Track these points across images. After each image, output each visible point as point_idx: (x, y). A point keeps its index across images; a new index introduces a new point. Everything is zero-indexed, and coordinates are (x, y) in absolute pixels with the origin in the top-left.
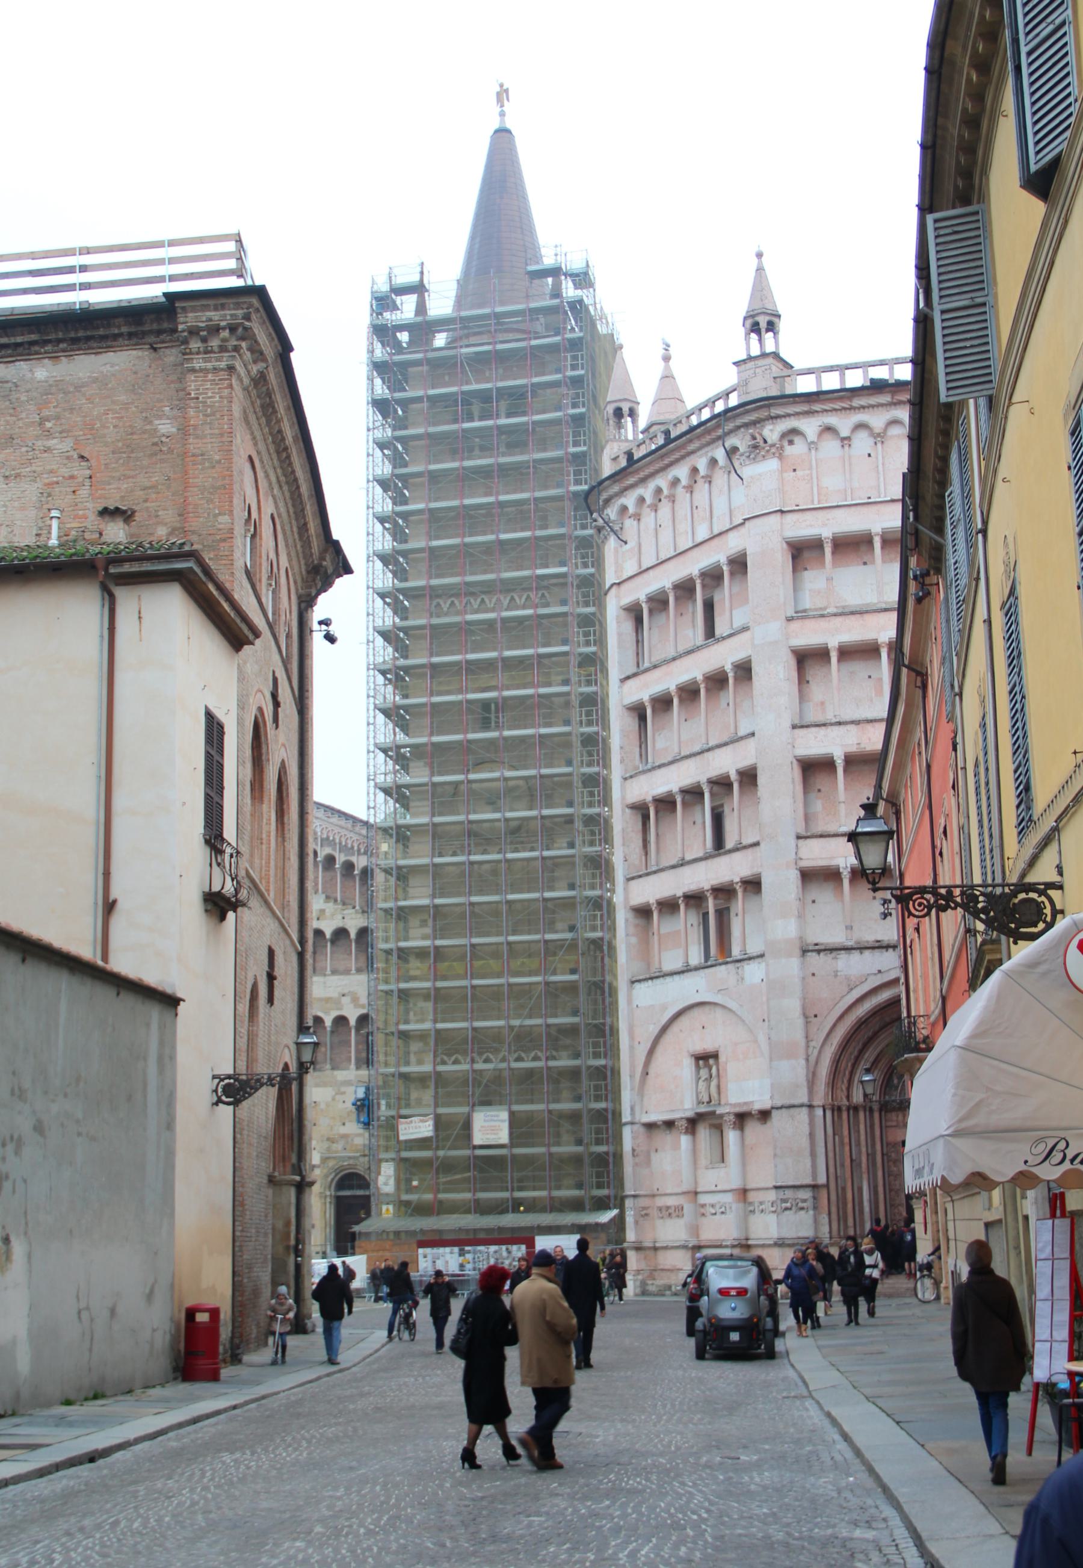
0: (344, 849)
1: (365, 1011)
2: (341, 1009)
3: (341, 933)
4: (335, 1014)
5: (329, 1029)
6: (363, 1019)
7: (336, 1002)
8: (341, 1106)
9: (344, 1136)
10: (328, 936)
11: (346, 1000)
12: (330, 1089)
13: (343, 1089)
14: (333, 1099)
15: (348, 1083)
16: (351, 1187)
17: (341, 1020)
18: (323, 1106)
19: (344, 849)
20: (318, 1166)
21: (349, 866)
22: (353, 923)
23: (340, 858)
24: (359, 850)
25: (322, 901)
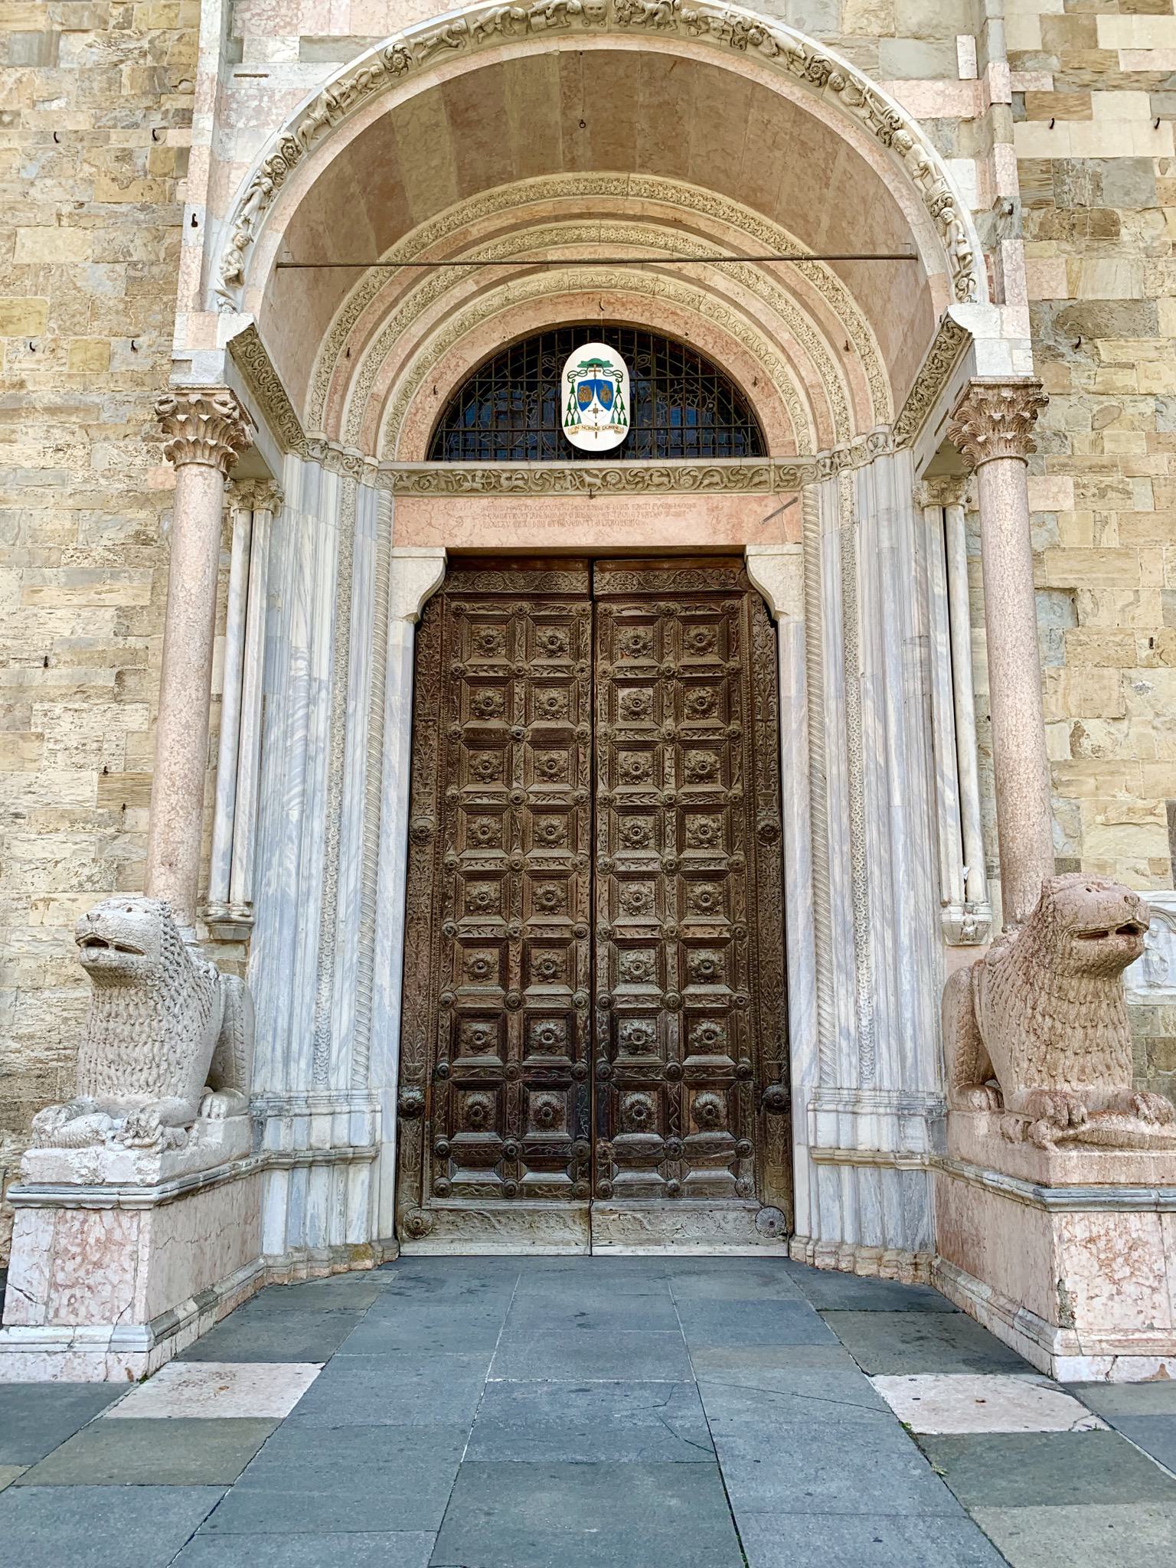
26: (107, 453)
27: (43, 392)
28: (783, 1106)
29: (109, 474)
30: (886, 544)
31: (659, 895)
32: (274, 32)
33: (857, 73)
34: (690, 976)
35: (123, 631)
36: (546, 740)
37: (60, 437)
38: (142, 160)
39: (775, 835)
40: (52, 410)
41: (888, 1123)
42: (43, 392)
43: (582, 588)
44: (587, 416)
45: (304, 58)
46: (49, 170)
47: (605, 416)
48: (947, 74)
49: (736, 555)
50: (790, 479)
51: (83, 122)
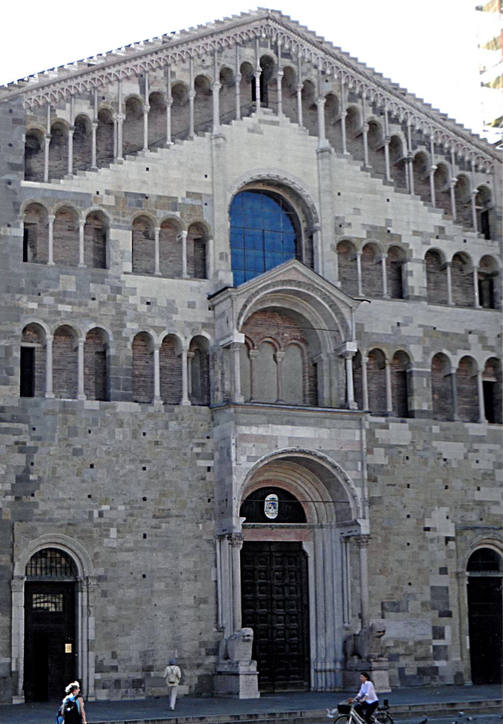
0: (460, 162)
2: (468, 349)
4: (462, 353)
7: (462, 340)
8: (474, 465)
9: (480, 503)
10: (449, 259)
12: (462, 444)
13: (476, 446)
14: (466, 458)
15: (481, 439)
18: (454, 465)
19: (460, 162)
20: (453, 539)
23: (454, 173)
24: (476, 166)
25: (440, 216)
26: (189, 526)
27: (174, 512)
28: (309, 662)
29: (189, 531)
30: (334, 548)
31: (285, 619)
32: (242, 455)
33: (342, 469)
34: (293, 636)
35: (195, 567)
36: (261, 585)
37: (179, 523)
38: (189, 455)
39: (307, 607)
40: (177, 516)
41: (332, 664)
42: (174, 512)
43: (268, 550)
44: (271, 511)
45: (248, 460)
46: (171, 457)
47: (274, 511)
48: (356, 469)
49: (300, 543)
50: (312, 527)
51: (174, 445)
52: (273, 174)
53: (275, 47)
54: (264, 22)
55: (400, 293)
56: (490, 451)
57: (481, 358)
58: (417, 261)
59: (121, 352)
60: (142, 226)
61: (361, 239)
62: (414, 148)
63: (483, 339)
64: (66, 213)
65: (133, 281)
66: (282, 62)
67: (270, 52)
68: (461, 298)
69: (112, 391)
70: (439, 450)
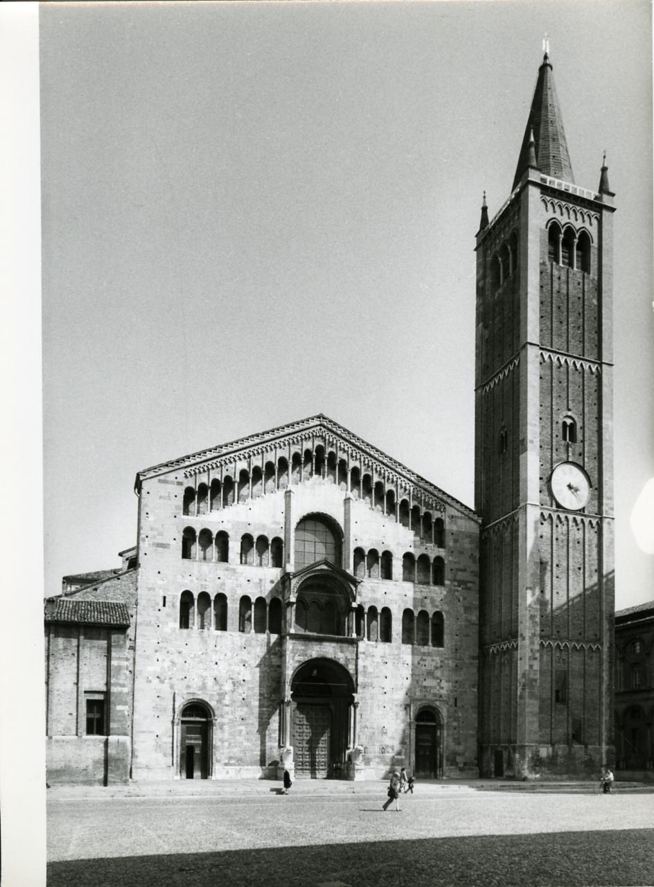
1: (438, 610)
3: (424, 558)
4: (420, 609)
5: (415, 618)
6: (438, 615)
9: (425, 687)
10: (416, 558)
11: (428, 601)
13: (424, 658)
14: (419, 663)
15: (429, 654)
16: (423, 721)
17: (423, 614)
21: (428, 516)
22: (433, 551)
23: (423, 510)
52: (321, 511)
53: (324, 439)
54: (319, 428)
55: (387, 575)
56: (433, 660)
57: (431, 611)
58: (398, 559)
59: (233, 607)
60: (247, 540)
61: (367, 547)
62: (401, 497)
63: (433, 601)
64: (206, 533)
65: (242, 569)
66: (329, 450)
67: (322, 444)
68: (422, 578)
69: (229, 627)
70: (404, 659)
